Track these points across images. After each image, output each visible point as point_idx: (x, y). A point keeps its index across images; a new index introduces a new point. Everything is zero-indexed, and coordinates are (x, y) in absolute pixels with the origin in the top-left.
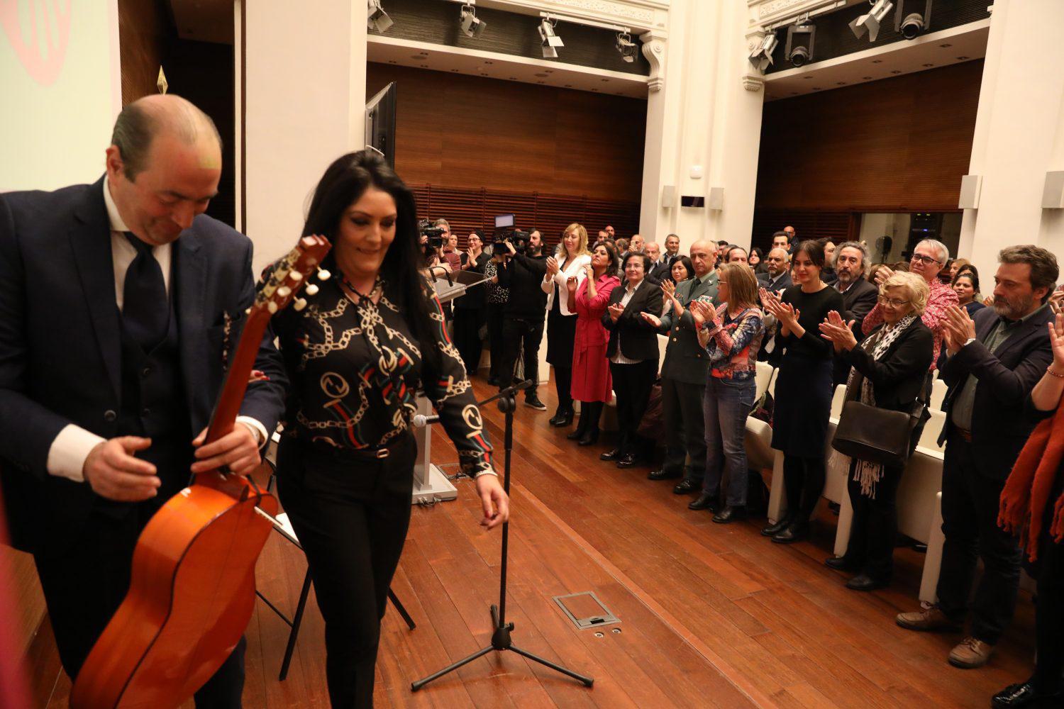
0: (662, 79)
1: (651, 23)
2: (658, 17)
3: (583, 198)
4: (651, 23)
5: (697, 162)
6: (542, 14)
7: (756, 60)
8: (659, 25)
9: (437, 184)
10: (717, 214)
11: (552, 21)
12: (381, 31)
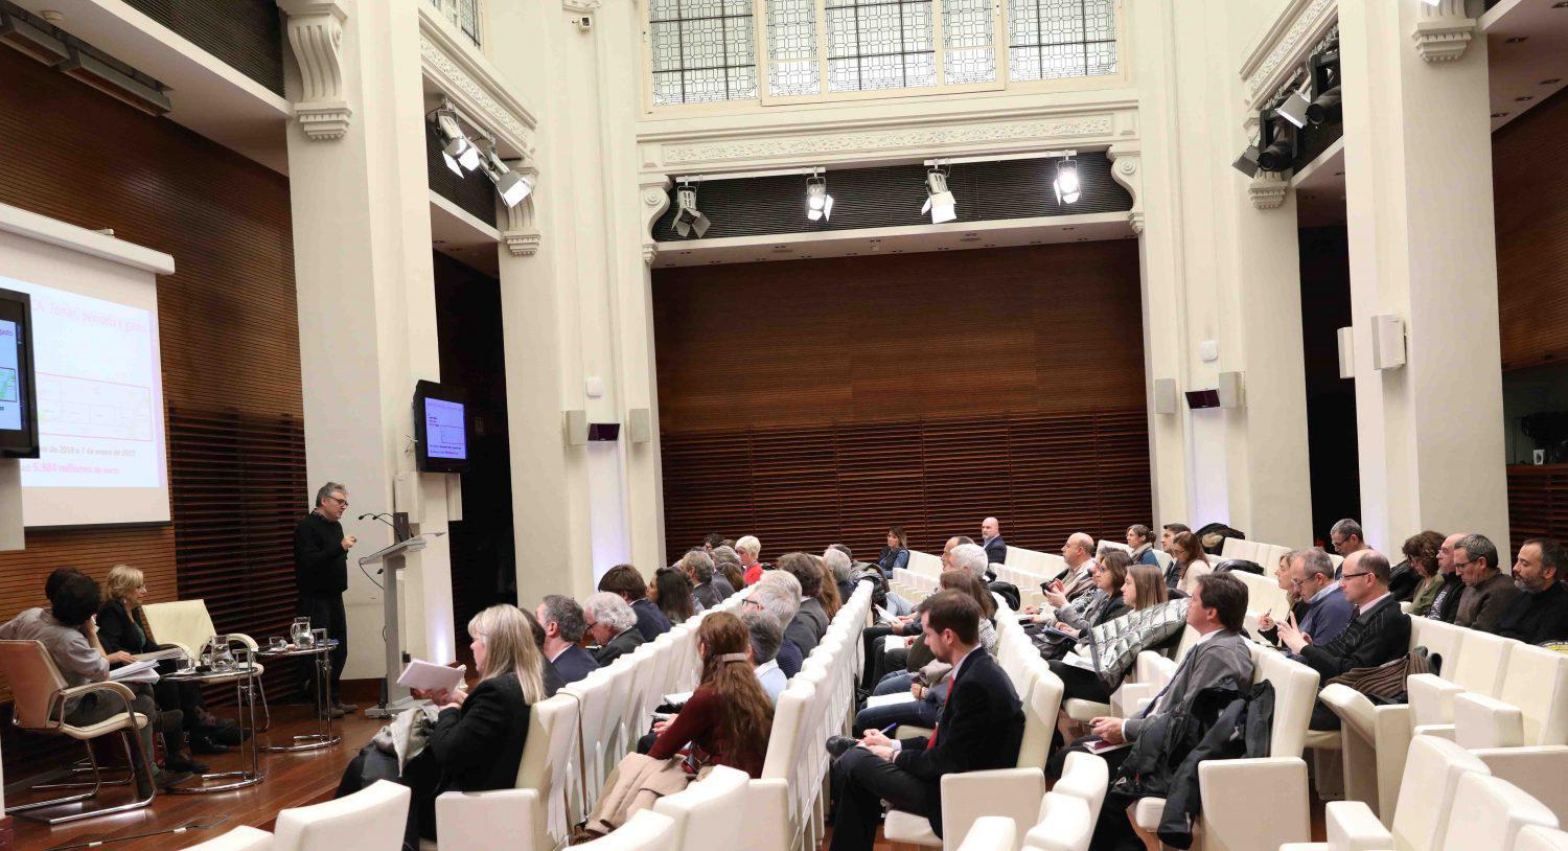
0: (1142, 214)
1: (1110, 134)
2: (1122, 121)
3: (1092, 412)
4: (1110, 134)
5: (1209, 335)
6: (927, 163)
7: (1243, 164)
8: (1123, 134)
9: (848, 420)
10: (1239, 413)
11: (943, 169)
12: (700, 233)
